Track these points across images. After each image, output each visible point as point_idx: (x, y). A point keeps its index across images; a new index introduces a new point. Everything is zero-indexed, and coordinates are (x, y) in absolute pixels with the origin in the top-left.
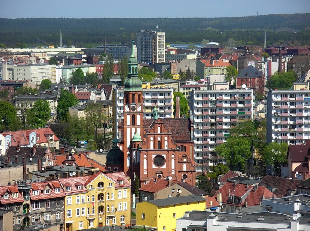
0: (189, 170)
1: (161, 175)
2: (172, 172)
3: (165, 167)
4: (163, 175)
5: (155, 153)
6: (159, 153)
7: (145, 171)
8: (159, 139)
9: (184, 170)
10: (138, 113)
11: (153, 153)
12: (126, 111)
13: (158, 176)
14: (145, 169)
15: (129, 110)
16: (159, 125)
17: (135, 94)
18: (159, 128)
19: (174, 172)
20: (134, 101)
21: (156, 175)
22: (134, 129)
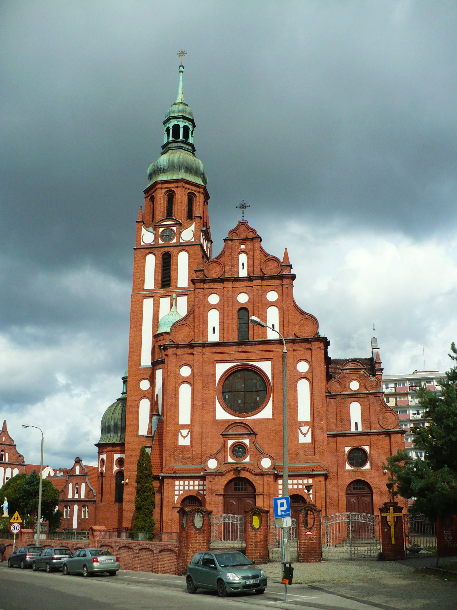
0: (373, 425)
1: (247, 442)
2: (300, 436)
3: (270, 416)
4: (252, 443)
5: (227, 357)
6: (243, 356)
7: (185, 432)
8: (243, 298)
9: (353, 429)
10: (184, 247)
11: (217, 357)
12: (142, 243)
13: (235, 446)
14: (184, 427)
15: (155, 238)
16: (243, 246)
17: (174, 189)
18: (243, 258)
19: (309, 435)
20: (170, 214)
21: (226, 443)
22: (168, 299)
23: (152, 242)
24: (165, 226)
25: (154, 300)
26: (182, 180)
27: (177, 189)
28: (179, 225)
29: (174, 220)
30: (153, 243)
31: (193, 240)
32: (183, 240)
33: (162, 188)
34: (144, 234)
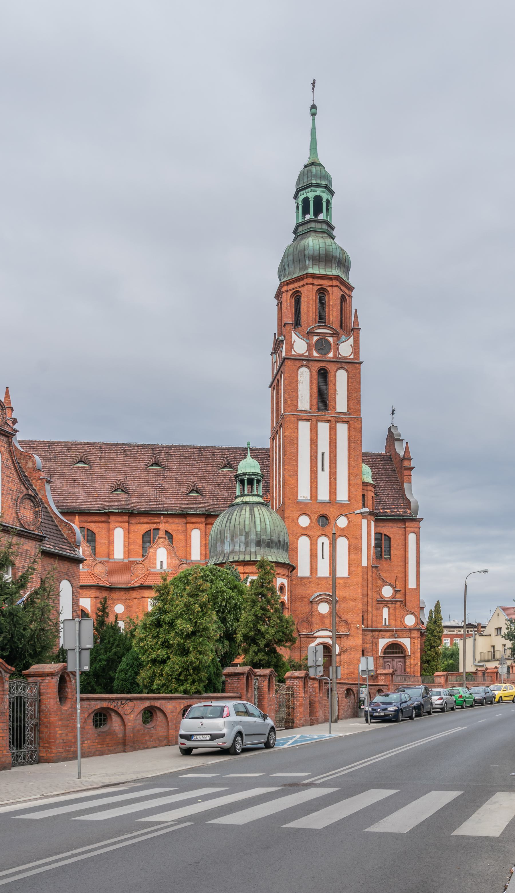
12: (293, 353)
15: (309, 349)
17: (328, 289)
22: (327, 425)
23: (305, 353)
24: (320, 335)
25: (311, 424)
26: (338, 278)
27: (331, 288)
28: (335, 335)
29: (328, 328)
30: (307, 354)
31: (352, 357)
32: (341, 355)
33: (313, 284)
34: (295, 341)
